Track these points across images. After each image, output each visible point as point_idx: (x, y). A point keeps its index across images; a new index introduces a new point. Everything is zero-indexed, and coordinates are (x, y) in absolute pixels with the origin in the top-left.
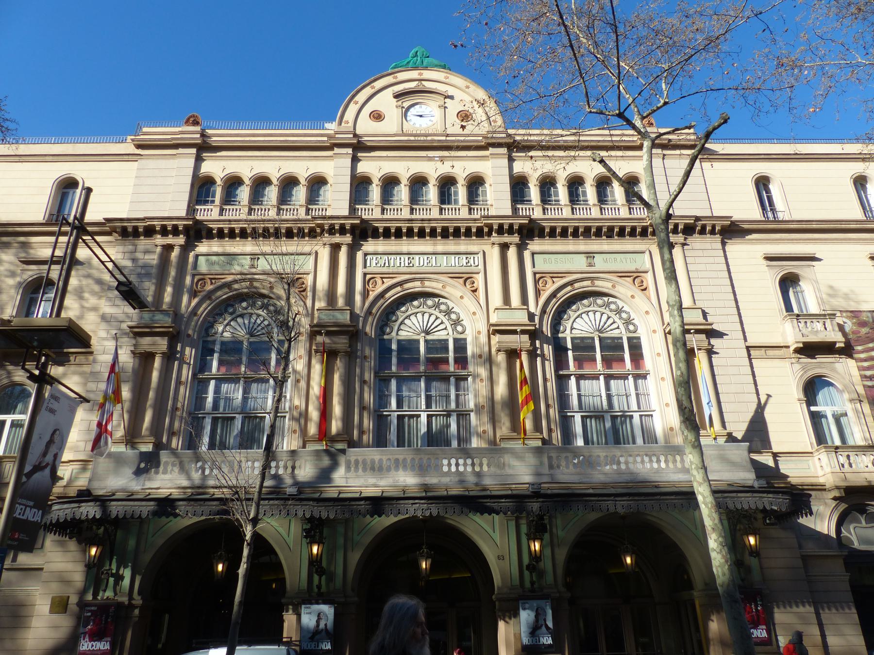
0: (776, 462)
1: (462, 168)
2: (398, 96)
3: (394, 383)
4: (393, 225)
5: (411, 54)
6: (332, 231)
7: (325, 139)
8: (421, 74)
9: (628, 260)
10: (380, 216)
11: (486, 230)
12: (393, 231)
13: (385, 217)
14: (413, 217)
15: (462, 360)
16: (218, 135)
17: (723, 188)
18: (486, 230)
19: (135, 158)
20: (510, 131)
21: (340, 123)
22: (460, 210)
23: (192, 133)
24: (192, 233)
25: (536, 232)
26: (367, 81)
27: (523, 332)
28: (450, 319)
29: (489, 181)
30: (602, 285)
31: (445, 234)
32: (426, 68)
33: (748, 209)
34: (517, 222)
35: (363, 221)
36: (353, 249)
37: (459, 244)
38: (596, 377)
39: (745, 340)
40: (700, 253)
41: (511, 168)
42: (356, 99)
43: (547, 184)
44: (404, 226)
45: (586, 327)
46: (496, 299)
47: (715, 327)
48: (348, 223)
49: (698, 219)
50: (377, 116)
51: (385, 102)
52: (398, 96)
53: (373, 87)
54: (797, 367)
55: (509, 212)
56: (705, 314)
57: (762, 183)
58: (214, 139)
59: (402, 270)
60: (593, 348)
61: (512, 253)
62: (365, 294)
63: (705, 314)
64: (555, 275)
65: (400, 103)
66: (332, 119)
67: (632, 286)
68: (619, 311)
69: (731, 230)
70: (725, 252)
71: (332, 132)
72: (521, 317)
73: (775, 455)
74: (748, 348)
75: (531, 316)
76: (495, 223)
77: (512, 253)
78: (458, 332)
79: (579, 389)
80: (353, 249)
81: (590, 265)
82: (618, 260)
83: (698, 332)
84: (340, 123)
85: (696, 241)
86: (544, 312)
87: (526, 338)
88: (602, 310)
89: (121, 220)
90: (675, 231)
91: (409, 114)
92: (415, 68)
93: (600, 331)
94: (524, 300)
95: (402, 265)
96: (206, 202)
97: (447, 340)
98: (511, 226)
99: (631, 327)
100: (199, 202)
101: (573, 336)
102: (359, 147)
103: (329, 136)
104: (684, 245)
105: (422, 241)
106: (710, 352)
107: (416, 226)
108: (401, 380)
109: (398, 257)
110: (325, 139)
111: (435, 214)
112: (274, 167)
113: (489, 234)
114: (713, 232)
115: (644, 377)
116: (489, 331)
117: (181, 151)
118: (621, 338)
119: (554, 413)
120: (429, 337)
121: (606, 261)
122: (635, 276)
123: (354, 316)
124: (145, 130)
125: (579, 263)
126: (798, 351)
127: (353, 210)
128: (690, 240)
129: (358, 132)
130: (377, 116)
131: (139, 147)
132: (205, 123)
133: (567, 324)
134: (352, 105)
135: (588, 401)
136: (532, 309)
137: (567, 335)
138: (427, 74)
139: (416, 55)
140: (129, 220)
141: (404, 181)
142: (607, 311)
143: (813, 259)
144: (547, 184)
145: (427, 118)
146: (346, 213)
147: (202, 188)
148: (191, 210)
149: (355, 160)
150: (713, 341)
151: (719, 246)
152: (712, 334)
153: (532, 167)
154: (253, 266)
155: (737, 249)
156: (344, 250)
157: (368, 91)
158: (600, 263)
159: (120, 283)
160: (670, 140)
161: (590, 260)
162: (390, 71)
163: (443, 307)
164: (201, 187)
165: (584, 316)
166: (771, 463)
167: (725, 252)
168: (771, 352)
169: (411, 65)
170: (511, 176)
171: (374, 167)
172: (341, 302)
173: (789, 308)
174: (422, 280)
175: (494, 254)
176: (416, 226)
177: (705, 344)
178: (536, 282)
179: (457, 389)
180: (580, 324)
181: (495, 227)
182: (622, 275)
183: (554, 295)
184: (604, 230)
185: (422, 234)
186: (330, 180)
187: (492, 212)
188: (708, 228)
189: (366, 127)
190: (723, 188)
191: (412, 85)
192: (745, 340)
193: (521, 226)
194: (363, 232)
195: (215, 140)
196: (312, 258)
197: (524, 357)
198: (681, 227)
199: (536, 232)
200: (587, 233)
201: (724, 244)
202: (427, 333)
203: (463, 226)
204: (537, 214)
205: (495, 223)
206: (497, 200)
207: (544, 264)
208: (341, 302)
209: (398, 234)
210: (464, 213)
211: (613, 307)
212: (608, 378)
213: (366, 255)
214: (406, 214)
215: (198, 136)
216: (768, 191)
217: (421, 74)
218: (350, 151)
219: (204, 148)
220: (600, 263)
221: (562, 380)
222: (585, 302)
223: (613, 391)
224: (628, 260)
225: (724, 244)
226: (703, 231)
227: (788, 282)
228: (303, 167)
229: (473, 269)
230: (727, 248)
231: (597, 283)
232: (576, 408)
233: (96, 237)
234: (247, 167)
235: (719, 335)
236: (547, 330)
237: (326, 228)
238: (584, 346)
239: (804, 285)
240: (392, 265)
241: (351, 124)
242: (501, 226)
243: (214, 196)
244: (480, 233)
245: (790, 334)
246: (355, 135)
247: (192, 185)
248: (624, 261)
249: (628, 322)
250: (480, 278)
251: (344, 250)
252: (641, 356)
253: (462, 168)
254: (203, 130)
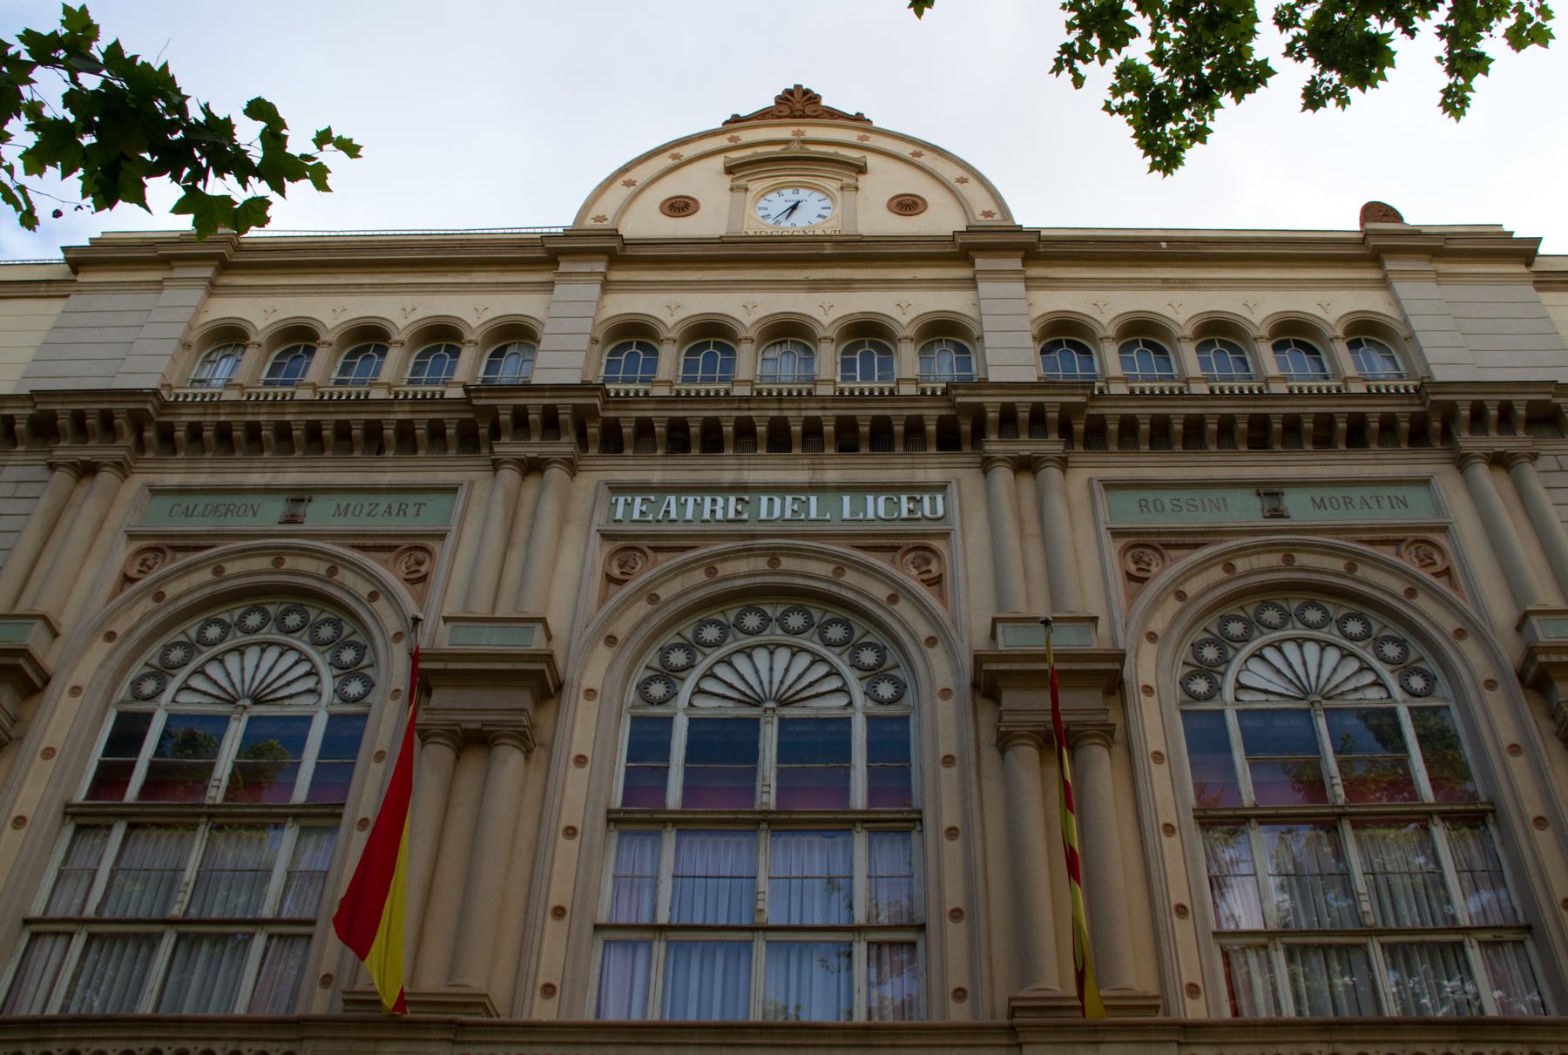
9: (1385, 503)
11: (966, 427)
12: (695, 430)
18: (966, 427)
31: (848, 439)
37: (889, 466)
45: (1277, 685)
53: (675, 157)
65: (743, 182)
76: (993, 403)
78: (880, 702)
81: (1277, 513)
82: (1356, 501)
95: (719, 515)
97: (847, 721)
101: (1241, 706)
105: (778, 458)
109: (708, 499)
116: (975, 685)
117: (178, 273)
118: (1392, 713)
120: (789, 712)
121: (1320, 505)
154: (291, 519)
158: (1299, 508)
161: (1269, 503)
165: (1270, 654)
181: (993, 415)
185: (779, 439)
200: (1260, 435)
202: (784, 703)
203: (898, 415)
224: (1385, 503)
237: (505, 417)
240: (689, 516)
248: (1373, 503)
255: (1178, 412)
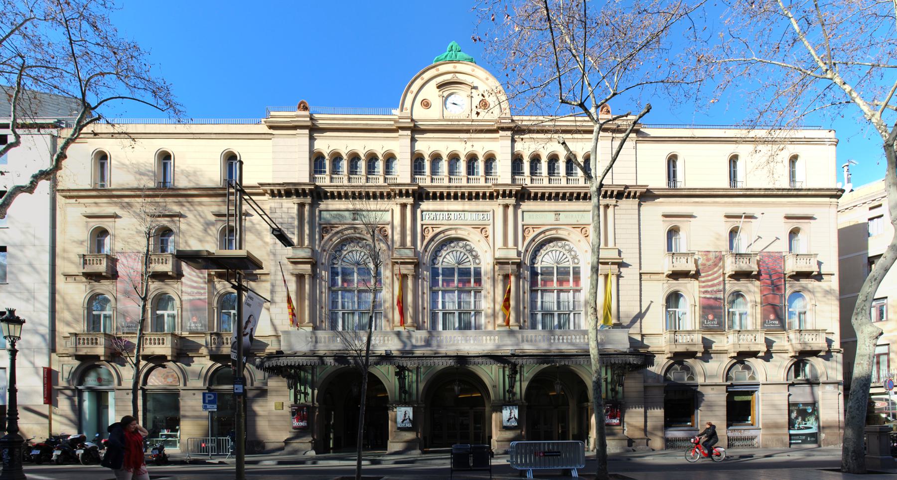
0: (642, 339)
1: (481, 146)
2: (440, 86)
3: (440, 293)
4: (438, 191)
5: (448, 49)
6: (401, 194)
7: (392, 123)
8: (455, 67)
10: (430, 184)
11: (495, 194)
13: (433, 184)
14: (451, 184)
15: (478, 281)
16: (323, 119)
17: (643, 165)
18: (495, 194)
19: (269, 137)
20: (515, 118)
21: (402, 110)
22: (480, 181)
23: (302, 117)
24: (315, 194)
25: (526, 196)
26: (418, 73)
27: (513, 263)
28: (472, 255)
29: (498, 157)
30: (562, 234)
32: (458, 62)
33: (657, 180)
34: (515, 189)
35: (420, 187)
36: (415, 206)
38: (552, 291)
39: (640, 269)
40: (624, 212)
41: (513, 147)
42: (412, 88)
43: (535, 160)
44: (445, 191)
46: (499, 242)
47: (625, 261)
48: (411, 188)
49: (627, 187)
50: (426, 104)
51: (431, 92)
52: (440, 86)
53: (422, 79)
54: (666, 285)
55: (509, 182)
56: (620, 253)
57: (672, 160)
58: (320, 122)
59: (444, 222)
60: (552, 274)
61: (511, 210)
62: (423, 237)
63: (620, 253)
64: (535, 226)
66: (396, 107)
67: (579, 233)
68: (570, 251)
69: (647, 195)
70: (639, 210)
71: (396, 117)
72: (512, 254)
73: (643, 336)
74: (641, 274)
75: (519, 254)
76: (501, 189)
77: (511, 210)
79: (542, 298)
80: (415, 206)
83: (613, 263)
84: (402, 110)
85: (624, 203)
86: (526, 251)
87: (515, 267)
88: (561, 249)
89: (269, 184)
90: (611, 196)
91: (448, 102)
92: (451, 62)
93: (558, 263)
94: (516, 243)
96: (321, 172)
98: (511, 191)
99: (576, 261)
100: (316, 172)
102: (416, 130)
103: (396, 122)
104: (615, 206)
105: (456, 202)
106: (619, 276)
107: (452, 191)
108: (444, 292)
110: (392, 123)
111: (464, 182)
112: (362, 145)
113: (497, 197)
114: (634, 197)
115: (579, 291)
117: (299, 131)
119: (527, 311)
122: (582, 227)
123: (416, 253)
124: (272, 113)
125: (550, 218)
126: (669, 276)
127: (413, 179)
128: (620, 202)
129: (414, 118)
130: (426, 104)
131: (271, 127)
132: (312, 109)
133: (539, 258)
134: (409, 94)
135: (547, 305)
136: (520, 249)
137: (538, 266)
138: (460, 67)
139: (451, 50)
140: (274, 185)
141: (445, 158)
142: (563, 251)
143: (691, 216)
144: (535, 160)
145: (461, 107)
146: (409, 181)
147: (317, 161)
148: (312, 178)
149: (413, 140)
150: (622, 269)
151: (637, 207)
152: (621, 265)
153: (526, 147)
155: (648, 208)
156: (409, 208)
157: (419, 83)
158: (564, 218)
159: (274, 229)
160: (619, 126)
162: (434, 64)
163: (468, 248)
164: (316, 160)
166: (640, 339)
167: (639, 210)
168: (653, 277)
169: (448, 59)
170: (513, 154)
171: (426, 146)
172: (409, 244)
173: (669, 248)
174: (456, 229)
175: (499, 211)
176: (452, 191)
177: (616, 272)
178: (524, 231)
179: (475, 298)
180: (547, 259)
182: (575, 226)
183: (533, 240)
184: (568, 195)
185: (456, 197)
186: (397, 156)
187: (499, 182)
188: (632, 194)
189: (420, 113)
190: (643, 165)
191: (448, 77)
192: (640, 269)
193: (517, 191)
194: (420, 195)
195: (321, 123)
196: (390, 212)
197: (513, 279)
198: (615, 193)
199: (526, 196)
201: (640, 205)
203: (481, 191)
204: (528, 182)
205: (501, 189)
206: (503, 172)
207: (530, 219)
208: (409, 244)
209: (442, 197)
210: (482, 182)
211: (567, 247)
212: (559, 291)
213: (422, 212)
214: (446, 182)
215: (308, 119)
216: (674, 167)
217: (455, 67)
218: (409, 133)
219: (314, 130)
220: (564, 218)
221: (533, 291)
222: (551, 244)
223: (561, 300)
225: (640, 205)
226: (628, 197)
227: (673, 232)
228: (379, 145)
229: (487, 222)
230: (642, 208)
231: (559, 232)
232: (539, 309)
233: (254, 198)
234: (344, 145)
235: (626, 265)
236: (528, 262)
238: (547, 272)
239: (682, 234)
241: (409, 111)
242: (504, 191)
243: (325, 168)
244: (491, 197)
245: (667, 265)
246: (412, 120)
247: (310, 159)
249: (575, 257)
250: (490, 229)
251: (409, 208)
252: (579, 278)
253: (481, 146)
254: (311, 114)
255: (540, 191)
